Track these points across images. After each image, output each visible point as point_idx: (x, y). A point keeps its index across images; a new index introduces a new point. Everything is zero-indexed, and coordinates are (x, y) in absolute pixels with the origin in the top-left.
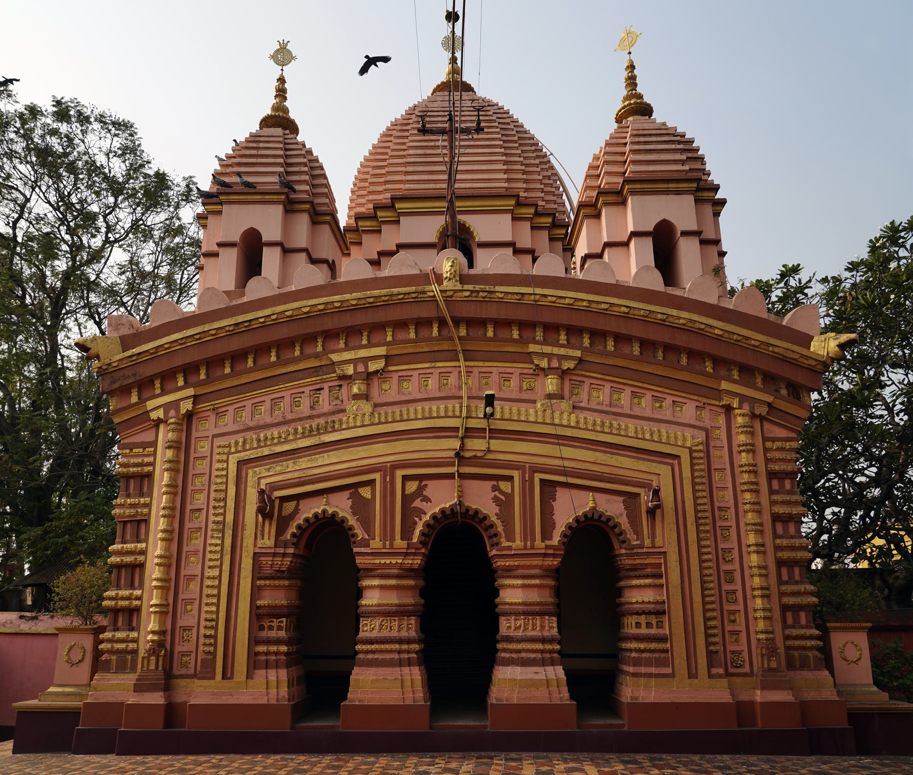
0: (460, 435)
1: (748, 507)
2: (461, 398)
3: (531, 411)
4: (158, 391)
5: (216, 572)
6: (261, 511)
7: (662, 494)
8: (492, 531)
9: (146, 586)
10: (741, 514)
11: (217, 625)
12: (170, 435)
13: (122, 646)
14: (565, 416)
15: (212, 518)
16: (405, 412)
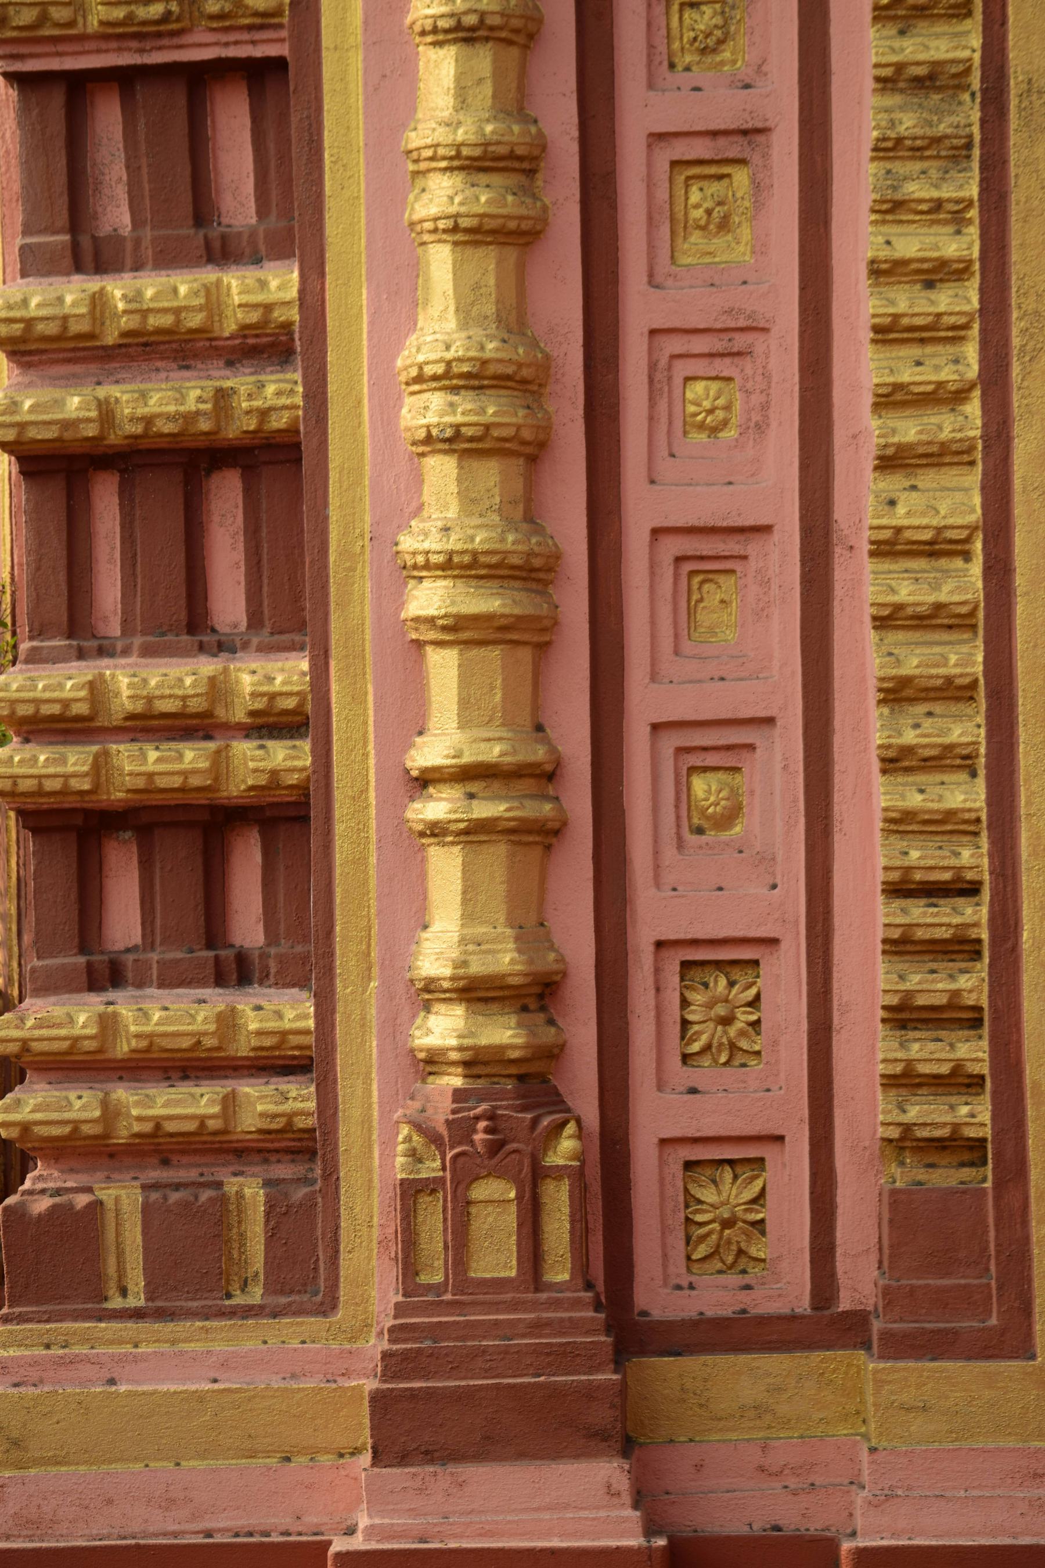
13: (193, 1103)
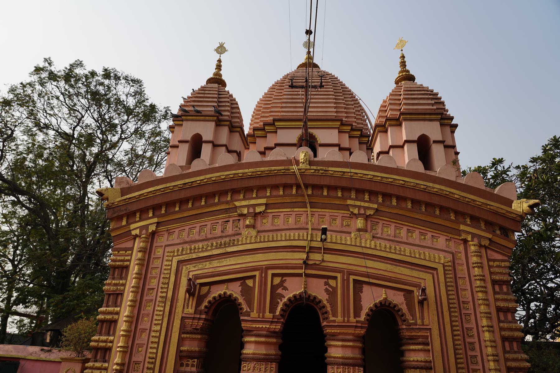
0: (307, 250)
1: (480, 302)
2: (308, 229)
3: (348, 238)
4: (138, 219)
5: (158, 328)
6: (188, 291)
7: (427, 291)
8: (324, 310)
9: (117, 334)
10: (477, 306)
11: (156, 361)
12: (142, 244)
14: (368, 242)
15: (160, 294)
16: (275, 236)
